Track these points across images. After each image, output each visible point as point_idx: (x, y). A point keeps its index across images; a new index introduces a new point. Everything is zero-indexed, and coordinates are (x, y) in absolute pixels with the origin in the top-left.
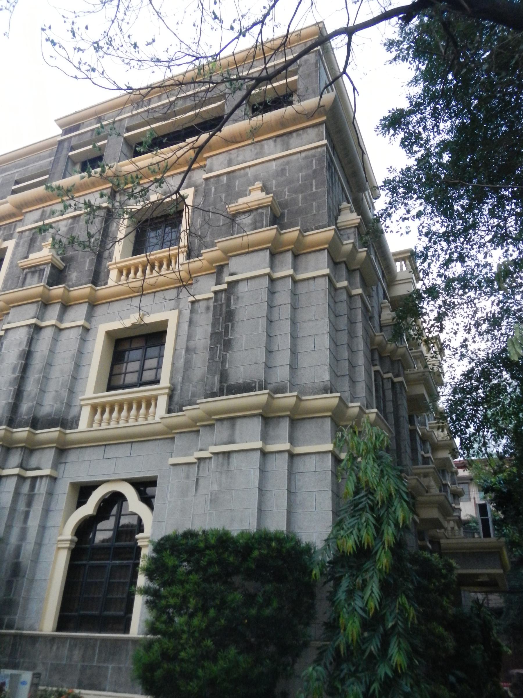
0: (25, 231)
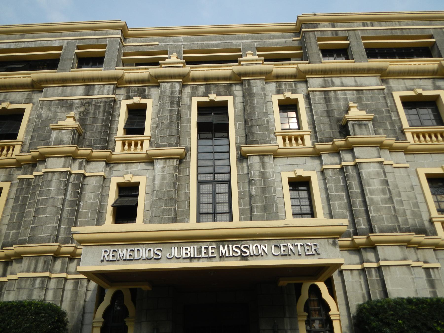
0: (316, 91)
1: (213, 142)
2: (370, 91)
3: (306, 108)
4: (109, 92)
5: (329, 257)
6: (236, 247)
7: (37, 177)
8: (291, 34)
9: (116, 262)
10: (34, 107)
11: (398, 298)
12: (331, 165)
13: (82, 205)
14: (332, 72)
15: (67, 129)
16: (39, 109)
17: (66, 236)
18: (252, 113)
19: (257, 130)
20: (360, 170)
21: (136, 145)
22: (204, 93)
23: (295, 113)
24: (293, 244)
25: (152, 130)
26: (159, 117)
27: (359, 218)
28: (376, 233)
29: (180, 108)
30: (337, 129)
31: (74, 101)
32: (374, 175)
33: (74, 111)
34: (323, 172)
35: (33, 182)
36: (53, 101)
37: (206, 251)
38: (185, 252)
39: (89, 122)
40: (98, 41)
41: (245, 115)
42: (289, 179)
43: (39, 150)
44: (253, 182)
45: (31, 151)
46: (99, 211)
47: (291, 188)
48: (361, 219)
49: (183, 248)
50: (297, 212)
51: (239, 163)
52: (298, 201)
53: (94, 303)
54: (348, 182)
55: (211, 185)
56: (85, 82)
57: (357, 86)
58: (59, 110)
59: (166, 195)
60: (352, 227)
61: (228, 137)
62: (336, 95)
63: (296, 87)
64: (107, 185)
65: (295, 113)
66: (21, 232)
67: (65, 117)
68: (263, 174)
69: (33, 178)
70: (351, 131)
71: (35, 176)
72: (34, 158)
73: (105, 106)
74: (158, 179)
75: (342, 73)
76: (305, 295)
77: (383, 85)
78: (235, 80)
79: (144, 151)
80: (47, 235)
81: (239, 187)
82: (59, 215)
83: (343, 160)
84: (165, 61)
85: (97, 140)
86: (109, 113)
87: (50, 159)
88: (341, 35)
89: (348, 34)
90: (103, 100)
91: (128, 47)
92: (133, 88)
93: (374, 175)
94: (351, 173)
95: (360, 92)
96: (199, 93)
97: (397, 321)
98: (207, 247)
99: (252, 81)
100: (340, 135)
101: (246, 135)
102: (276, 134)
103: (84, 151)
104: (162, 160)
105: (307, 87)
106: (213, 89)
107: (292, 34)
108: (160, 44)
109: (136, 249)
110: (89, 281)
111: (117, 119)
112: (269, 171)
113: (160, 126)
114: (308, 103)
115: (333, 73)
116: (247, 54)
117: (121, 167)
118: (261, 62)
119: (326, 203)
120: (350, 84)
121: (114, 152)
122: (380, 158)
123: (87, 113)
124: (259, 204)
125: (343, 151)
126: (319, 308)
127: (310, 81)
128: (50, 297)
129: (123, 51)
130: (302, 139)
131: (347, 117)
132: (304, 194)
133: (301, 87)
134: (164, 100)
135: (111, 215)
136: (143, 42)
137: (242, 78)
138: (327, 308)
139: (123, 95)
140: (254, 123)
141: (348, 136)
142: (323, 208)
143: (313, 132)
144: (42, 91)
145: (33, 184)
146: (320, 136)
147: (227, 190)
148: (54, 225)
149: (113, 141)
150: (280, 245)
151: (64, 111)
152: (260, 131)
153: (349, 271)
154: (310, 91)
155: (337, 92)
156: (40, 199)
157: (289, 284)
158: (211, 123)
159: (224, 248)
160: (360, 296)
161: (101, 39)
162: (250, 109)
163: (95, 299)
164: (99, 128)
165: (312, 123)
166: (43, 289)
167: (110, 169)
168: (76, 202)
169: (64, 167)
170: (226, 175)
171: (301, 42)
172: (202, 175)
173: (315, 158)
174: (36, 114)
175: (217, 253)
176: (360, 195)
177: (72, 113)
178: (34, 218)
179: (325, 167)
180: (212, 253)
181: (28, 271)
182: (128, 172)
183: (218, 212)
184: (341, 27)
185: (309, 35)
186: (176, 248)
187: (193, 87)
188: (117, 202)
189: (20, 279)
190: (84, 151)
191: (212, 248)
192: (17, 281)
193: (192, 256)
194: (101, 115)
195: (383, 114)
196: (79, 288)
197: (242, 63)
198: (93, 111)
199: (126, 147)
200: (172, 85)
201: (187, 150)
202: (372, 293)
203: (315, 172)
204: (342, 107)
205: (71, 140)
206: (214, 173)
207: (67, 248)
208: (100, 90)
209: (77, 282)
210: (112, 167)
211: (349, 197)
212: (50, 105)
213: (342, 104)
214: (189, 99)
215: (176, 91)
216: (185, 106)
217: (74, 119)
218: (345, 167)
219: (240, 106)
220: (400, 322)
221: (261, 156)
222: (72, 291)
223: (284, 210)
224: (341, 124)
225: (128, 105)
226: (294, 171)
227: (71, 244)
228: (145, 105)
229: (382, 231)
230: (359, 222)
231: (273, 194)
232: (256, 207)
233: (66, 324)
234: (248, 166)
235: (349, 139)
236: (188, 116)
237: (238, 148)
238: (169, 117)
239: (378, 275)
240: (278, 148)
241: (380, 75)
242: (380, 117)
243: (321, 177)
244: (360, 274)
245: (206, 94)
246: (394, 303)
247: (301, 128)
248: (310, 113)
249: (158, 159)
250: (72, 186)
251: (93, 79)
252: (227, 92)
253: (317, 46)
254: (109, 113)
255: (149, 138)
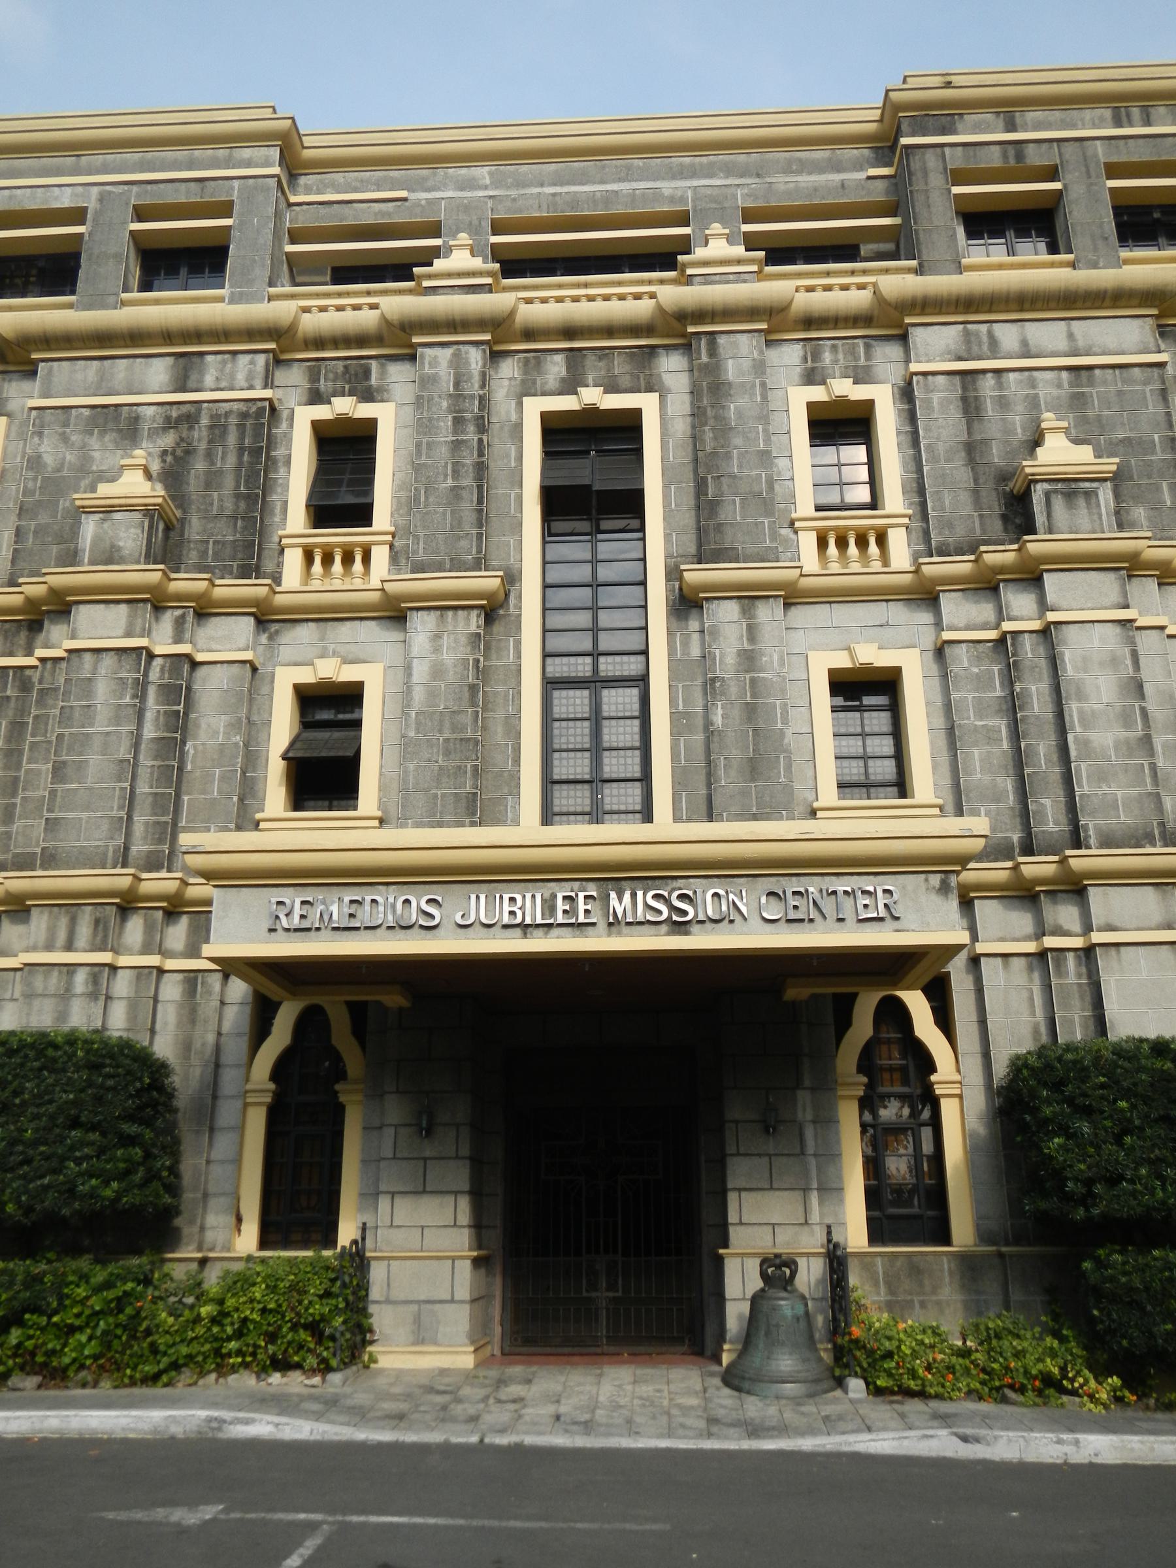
1: (594, 552)
2: (1117, 372)
3: (899, 433)
4: (253, 379)
5: (925, 927)
6: (657, 897)
7: (49, 665)
8: (862, 155)
9: (313, 933)
10: (14, 428)
11: (1130, 1039)
12: (968, 628)
13: (192, 752)
14: (992, 303)
15: (130, 508)
16: (32, 437)
17: (152, 848)
18: (719, 455)
19: (733, 513)
20: (1058, 649)
21: (348, 559)
22: (563, 380)
23: (864, 447)
24: (824, 888)
25: (397, 510)
26: (417, 468)
27: (1043, 801)
28: (1088, 847)
29: (485, 438)
30: (997, 508)
31: (140, 409)
32: (1101, 664)
33: (144, 445)
34: (940, 652)
35: (35, 679)
36: (73, 411)
37: (567, 908)
38: (507, 908)
39: (193, 486)
40: (202, 189)
41: (696, 460)
42: (832, 672)
43: (47, 578)
44: (718, 684)
45: (21, 580)
46: (244, 773)
47: (840, 701)
48: (1047, 802)
49: (501, 897)
50: (855, 779)
51: (675, 624)
52: (860, 743)
53: (246, 1038)
54: (1017, 688)
55: (586, 693)
56: (172, 344)
57: (1075, 353)
58: (94, 442)
59: (447, 724)
60: (1019, 827)
61: (642, 529)
62: (1000, 386)
63: (868, 357)
64: (265, 690)
65: (864, 447)
66: (17, 833)
67: (117, 467)
68: (749, 659)
69: (35, 667)
70: (1040, 519)
71: (43, 660)
72: (32, 604)
73: (241, 427)
74: (421, 672)
75: (1027, 305)
76: (863, 1026)
77: (1163, 347)
78: (668, 336)
79: (375, 582)
80: (97, 843)
81: (672, 701)
82: (127, 785)
83: (1008, 615)
84: (431, 264)
85: (224, 543)
86: (256, 452)
87: (83, 608)
88: (1035, 158)
89: (1060, 154)
90: (235, 406)
91: (305, 207)
92: (328, 363)
93: (1101, 664)
94: (1030, 655)
95: (1084, 373)
96: (546, 383)
97: (1115, 1101)
98: (573, 894)
99: (722, 340)
100: (1006, 530)
101: (699, 529)
102: (797, 524)
103: (186, 583)
104: (432, 613)
105: (908, 361)
106: (593, 368)
107: (866, 152)
108: (413, 196)
109: (368, 898)
110: (226, 977)
111: (282, 471)
112: (770, 649)
113: (422, 499)
114: (905, 414)
115: (994, 308)
116: (707, 235)
117: (305, 633)
118: (755, 268)
119: (945, 753)
120: (1050, 347)
121: (279, 584)
122: (1127, 607)
123: (188, 452)
124: (735, 754)
125: (1010, 585)
126: (904, 1062)
127: (918, 336)
128: (118, 1023)
129: (288, 224)
130: (882, 540)
131: (1028, 470)
132: (880, 721)
133: (887, 356)
134: (434, 409)
135: (280, 785)
136: (356, 190)
137: (691, 329)
138: (926, 1063)
139: (299, 390)
140: (725, 487)
141: (1026, 537)
142: (935, 767)
143: (918, 517)
144: (34, 373)
145: (37, 687)
146: (940, 533)
147: (635, 709)
148: (115, 813)
149: (275, 546)
150: (784, 892)
151: (111, 446)
152: (743, 516)
153: (999, 960)
154: (916, 374)
155: (1005, 375)
156: (63, 735)
157: (814, 996)
158: (588, 487)
159: (620, 899)
160: (1026, 1032)
161: (212, 183)
162: (715, 438)
163: (246, 1027)
164: (229, 504)
165: (915, 485)
166: (96, 999)
167: (271, 638)
168: (173, 745)
169: (129, 634)
170: (633, 658)
171: (896, 185)
172: (558, 660)
173: (919, 606)
174: (24, 453)
175: (599, 913)
176: (1052, 726)
177: (138, 452)
178: (53, 793)
179: (947, 635)
180: (587, 911)
181: (49, 947)
182: (325, 648)
183: (606, 776)
184: (1038, 127)
185: (924, 163)
186: (483, 897)
187: (527, 361)
188: (298, 745)
189: (27, 968)
190: (186, 583)
191: (586, 897)
192: (19, 974)
193: (528, 921)
194: (231, 461)
195: (1153, 452)
196: (198, 996)
197: (689, 271)
198: (203, 445)
199: (317, 567)
200: (456, 355)
201: (512, 578)
202: (1061, 1024)
203: (917, 651)
204: (1019, 431)
205: (144, 548)
206: (595, 654)
207: (159, 883)
208: (222, 370)
209: (192, 979)
210: (277, 632)
211: (1016, 734)
212: (66, 424)
213: (1018, 420)
214: (513, 403)
215: (470, 377)
216: (502, 428)
217: (148, 475)
218: (1013, 639)
219: (681, 427)
220: (1123, 1104)
221: (746, 601)
222: (181, 1006)
223: (810, 773)
224: (1012, 491)
225: (317, 426)
226: (848, 649)
227: (169, 871)
228: (372, 423)
229: (1108, 841)
230: (1041, 812)
231: (779, 725)
232: (725, 765)
233: (171, 1096)
234: (702, 632)
235: (1028, 545)
236: (513, 464)
237: (673, 574)
238: (450, 467)
239: (1084, 970)
240: (801, 575)
241: (1155, 312)
242: (1141, 463)
243: (934, 669)
244: (1030, 969)
245: (570, 387)
246: (1113, 1053)
247: (879, 506)
248: (911, 452)
249: (418, 609)
250: (158, 694)
251: (196, 334)
252: (639, 378)
253: (948, 204)
254: (256, 452)
255: (389, 538)
